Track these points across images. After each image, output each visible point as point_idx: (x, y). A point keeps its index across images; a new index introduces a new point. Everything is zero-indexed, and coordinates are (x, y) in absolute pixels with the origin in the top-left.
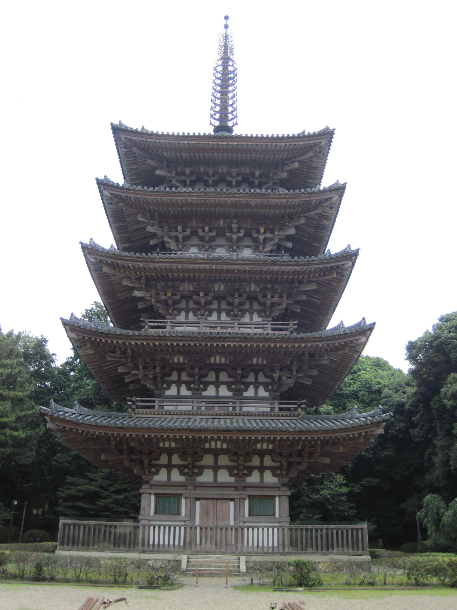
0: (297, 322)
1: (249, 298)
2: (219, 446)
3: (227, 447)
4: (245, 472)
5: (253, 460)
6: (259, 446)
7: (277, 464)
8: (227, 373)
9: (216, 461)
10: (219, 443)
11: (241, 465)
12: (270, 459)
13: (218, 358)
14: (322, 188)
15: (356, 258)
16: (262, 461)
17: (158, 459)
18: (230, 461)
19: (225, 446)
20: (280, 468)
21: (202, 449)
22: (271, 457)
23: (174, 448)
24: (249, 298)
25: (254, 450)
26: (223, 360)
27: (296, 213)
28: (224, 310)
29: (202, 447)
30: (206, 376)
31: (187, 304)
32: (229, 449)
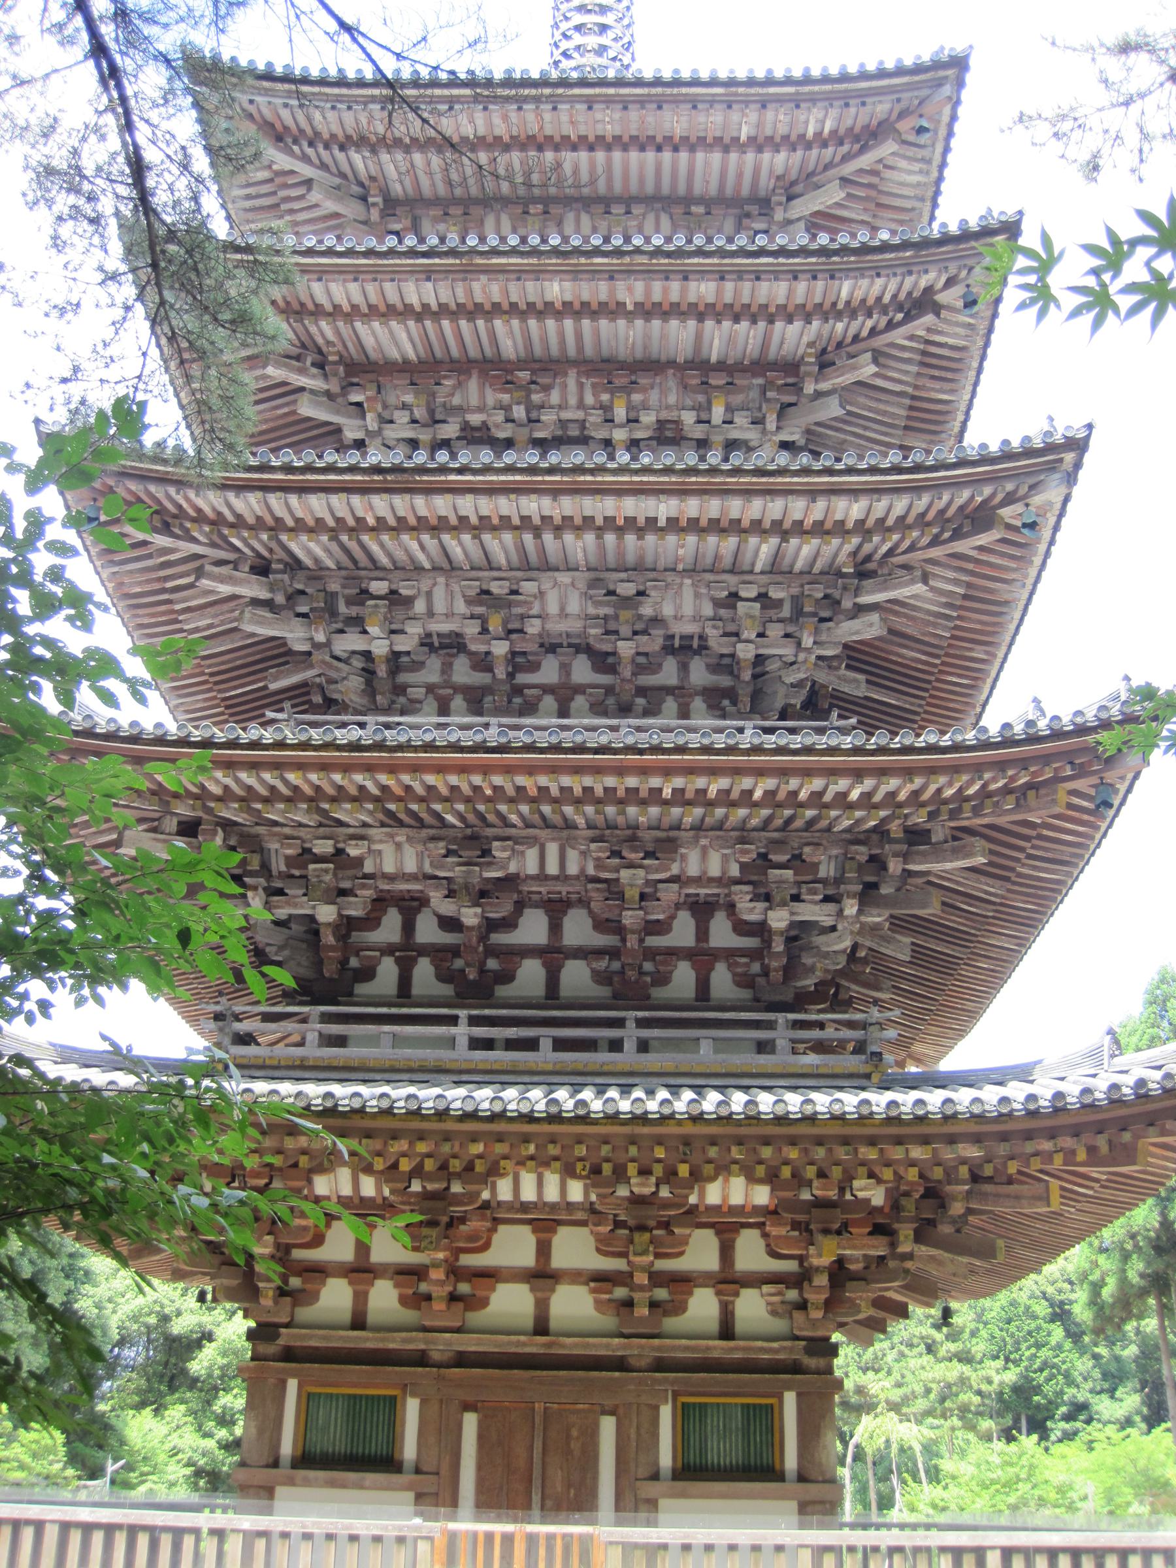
0: (853, 721)
1: (669, 649)
2: (552, 1194)
3: (586, 1194)
4: (662, 1294)
5: (689, 1250)
6: (713, 1194)
7: (791, 1266)
9: (544, 1250)
10: (552, 1180)
11: (643, 1269)
12: (762, 1243)
13: (552, 849)
14: (935, 231)
15: (1078, 465)
16: (727, 1252)
17: (318, 1240)
18: (598, 1250)
19: (576, 1191)
21: (486, 1205)
22: (765, 1235)
23: (372, 1200)
24: (669, 649)
25: (692, 1211)
26: (573, 856)
27: (840, 345)
28: (580, 689)
29: (486, 1195)
30: (509, 924)
31: (447, 668)
32: (592, 1203)
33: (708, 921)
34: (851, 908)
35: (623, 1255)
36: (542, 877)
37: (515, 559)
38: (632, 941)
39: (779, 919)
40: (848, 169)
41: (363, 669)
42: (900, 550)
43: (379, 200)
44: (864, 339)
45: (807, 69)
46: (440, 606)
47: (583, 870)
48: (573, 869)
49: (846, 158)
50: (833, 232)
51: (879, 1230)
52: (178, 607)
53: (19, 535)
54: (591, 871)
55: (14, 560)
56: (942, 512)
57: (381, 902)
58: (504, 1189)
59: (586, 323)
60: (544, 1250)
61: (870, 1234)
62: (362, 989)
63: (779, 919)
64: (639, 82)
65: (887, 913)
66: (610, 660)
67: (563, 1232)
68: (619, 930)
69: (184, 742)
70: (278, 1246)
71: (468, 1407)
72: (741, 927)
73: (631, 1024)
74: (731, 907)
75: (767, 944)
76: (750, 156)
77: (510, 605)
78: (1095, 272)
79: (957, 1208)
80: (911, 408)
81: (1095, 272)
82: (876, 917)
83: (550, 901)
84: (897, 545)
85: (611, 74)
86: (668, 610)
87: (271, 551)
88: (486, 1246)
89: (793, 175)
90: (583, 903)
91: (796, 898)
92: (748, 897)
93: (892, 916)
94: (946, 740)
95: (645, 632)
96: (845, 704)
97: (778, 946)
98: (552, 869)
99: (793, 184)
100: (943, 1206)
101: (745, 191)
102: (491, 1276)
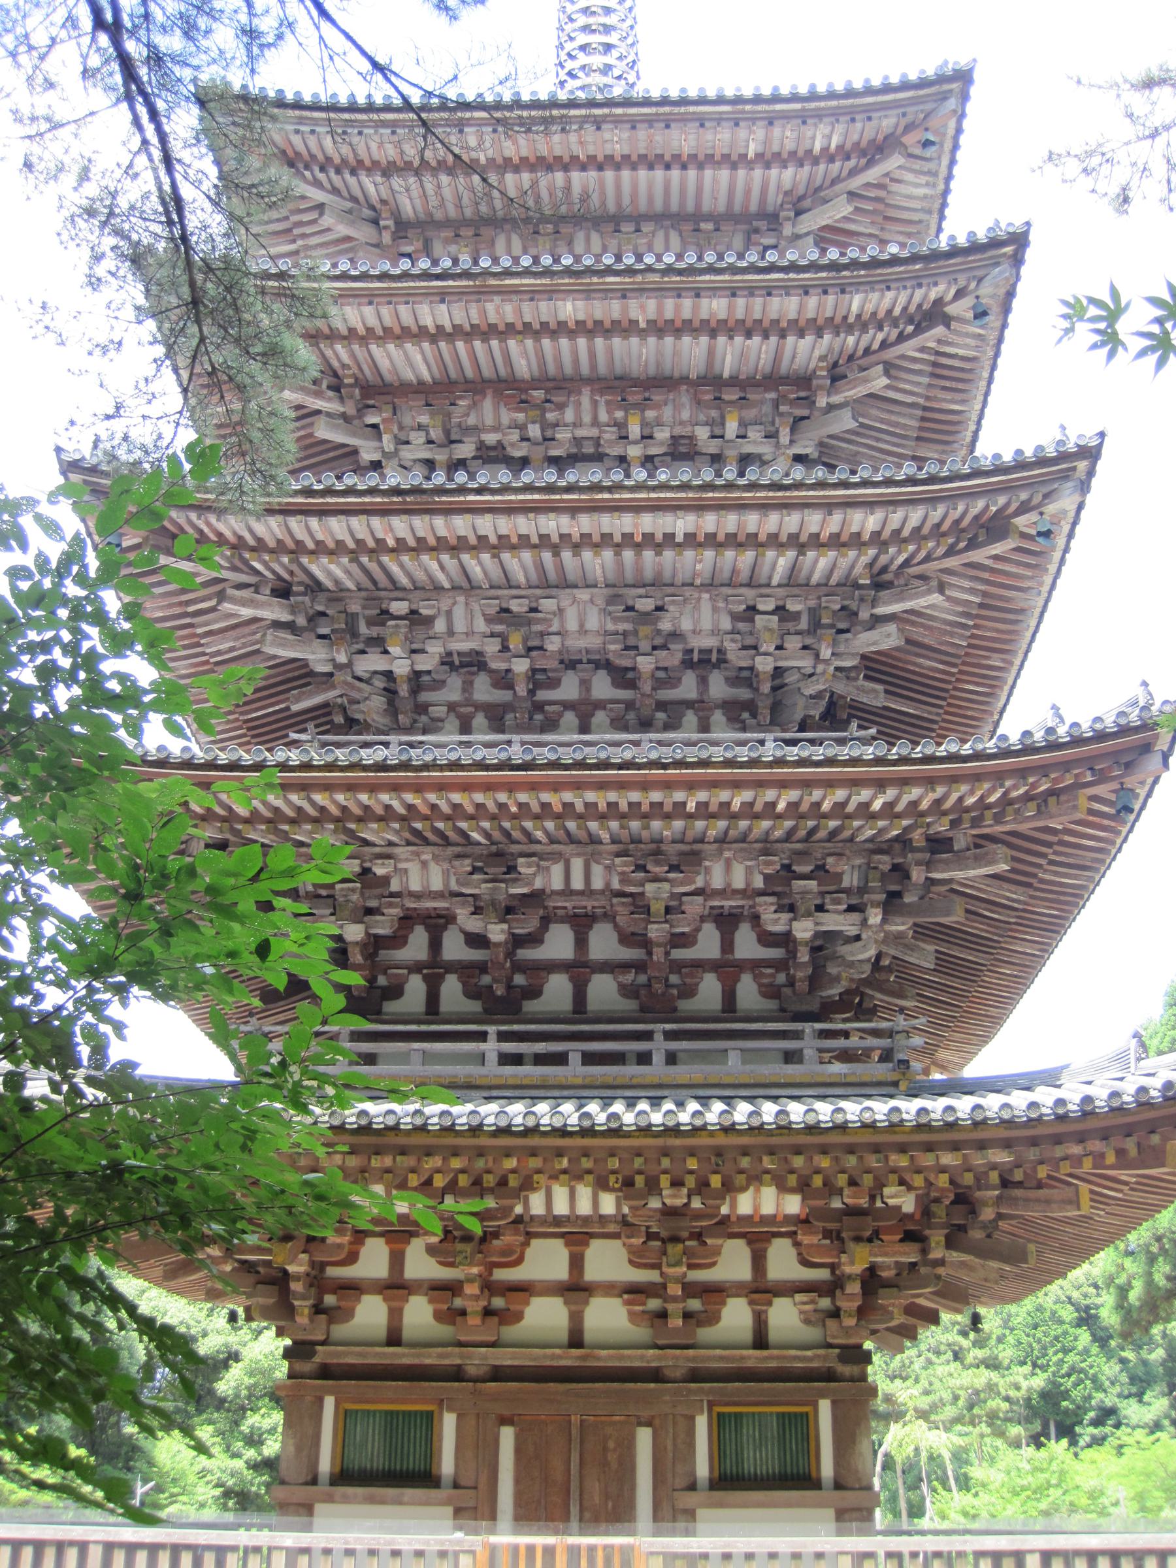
0: (873, 731)
2: (584, 1207)
3: (619, 1206)
4: (695, 1304)
5: (721, 1260)
6: (745, 1204)
7: (823, 1274)
8: (616, 926)
9: (577, 1263)
10: (584, 1193)
12: (793, 1252)
13: (577, 865)
14: (943, 243)
15: (1091, 473)
16: (759, 1261)
18: (631, 1262)
19: (608, 1204)
20: (832, 1287)
21: (519, 1220)
22: (797, 1244)
25: (725, 1221)
26: (597, 871)
27: (851, 358)
28: (600, 705)
29: (518, 1209)
30: (535, 939)
31: (468, 686)
32: (624, 1216)
33: (733, 933)
34: (875, 917)
35: (656, 1266)
36: (568, 892)
37: (534, 577)
38: (658, 954)
39: (803, 930)
40: (855, 183)
41: (385, 689)
42: (916, 561)
43: (390, 223)
44: (875, 352)
45: (813, 86)
46: (460, 626)
47: (608, 884)
48: (598, 884)
49: (853, 173)
50: (843, 246)
51: (910, 1237)
52: (199, 631)
53: (92, 574)
54: (616, 885)
55: (86, 598)
56: (957, 522)
57: (408, 920)
58: (537, 1204)
59: (599, 341)
60: (577, 1263)
61: (901, 1240)
62: (391, 1007)
63: (803, 930)
64: (647, 102)
65: (910, 922)
66: (630, 675)
67: (595, 1244)
68: (645, 943)
69: (211, 765)
70: (312, 1264)
71: (505, 1421)
72: (766, 939)
73: (659, 1037)
74: (755, 919)
75: (792, 954)
76: (758, 173)
77: (529, 623)
78: (1159, 321)
79: (987, 1214)
80: (923, 419)
81: (1159, 321)
82: (900, 926)
83: (576, 915)
84: (912, 556)
85: (618, 91)
86: (686, 625)
87: (291, 573)
88: (519, 1261)
89: (801, 190)
90: (610, 917)
91: (820, 908)
92: (773, 908)
93: (915, 925)
94: (966, 749)
95: (664, 647)
96: (864, 714)
97: (804, 956)
98: (577, 884)
99: (802, 198)
100: (973, 1212)
101: (753, 208)
102: (525, 1289)
